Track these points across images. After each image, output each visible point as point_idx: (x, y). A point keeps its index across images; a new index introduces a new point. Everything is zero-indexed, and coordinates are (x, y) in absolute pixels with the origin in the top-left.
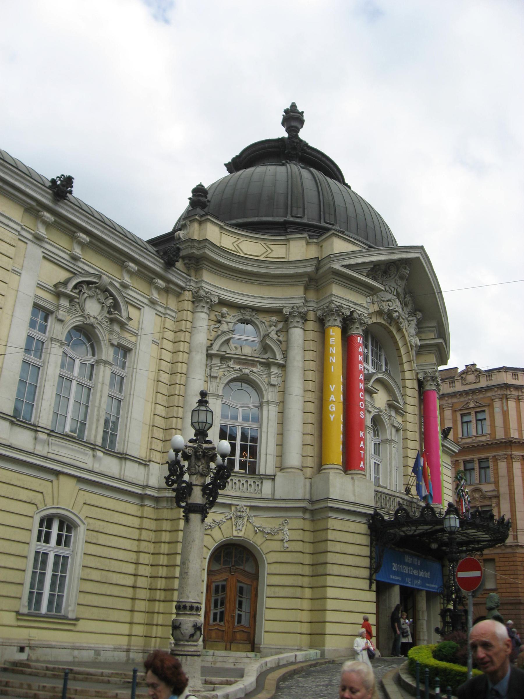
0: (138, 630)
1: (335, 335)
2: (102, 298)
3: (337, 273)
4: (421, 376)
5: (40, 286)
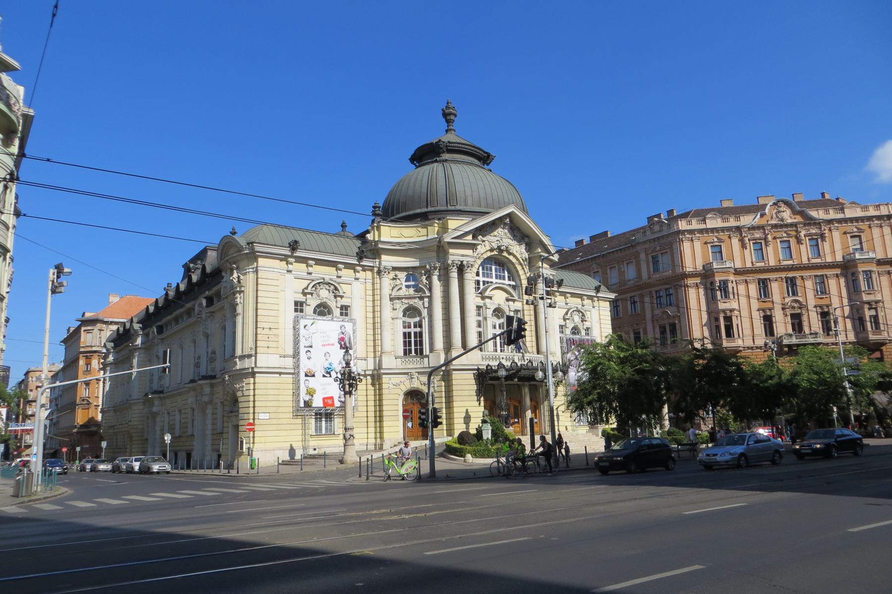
1: (454, 274)
2: (327, 287)
3: (449, 243)
5: (296, 292)
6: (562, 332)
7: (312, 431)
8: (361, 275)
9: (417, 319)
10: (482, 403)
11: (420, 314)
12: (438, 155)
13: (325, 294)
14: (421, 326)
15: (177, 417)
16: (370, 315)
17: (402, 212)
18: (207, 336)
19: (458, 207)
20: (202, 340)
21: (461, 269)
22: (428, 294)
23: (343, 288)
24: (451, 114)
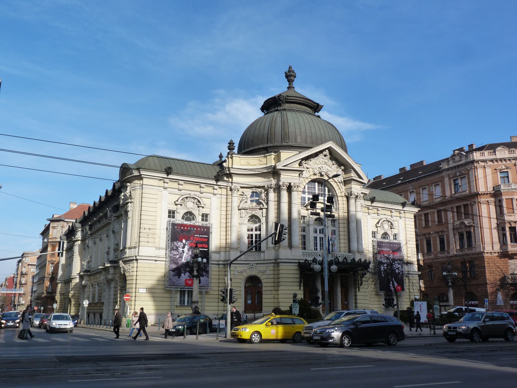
0: (220, 308)
1: (284, 194)
2: (193, 201)
4: (347, 194)
6: (375, 237)
7: (177, 303)
8: (219, 191)
9: (257, 225)
10: (302, 288)
11: (260, 221)
12: (280, 105)
13: (190, 205)
14: (260, 230)
15: (97, 289)
16: (224, 221)
17: (251, 147)
18: (113, 232)
19: (290, 144)
20: (112, 235)
21: (290, 189)
22: (266, 206)
23: (204, 201)
24: (291, 75)
